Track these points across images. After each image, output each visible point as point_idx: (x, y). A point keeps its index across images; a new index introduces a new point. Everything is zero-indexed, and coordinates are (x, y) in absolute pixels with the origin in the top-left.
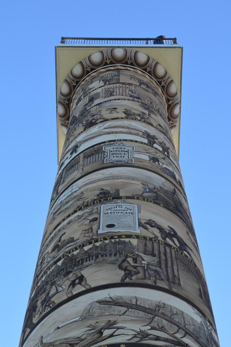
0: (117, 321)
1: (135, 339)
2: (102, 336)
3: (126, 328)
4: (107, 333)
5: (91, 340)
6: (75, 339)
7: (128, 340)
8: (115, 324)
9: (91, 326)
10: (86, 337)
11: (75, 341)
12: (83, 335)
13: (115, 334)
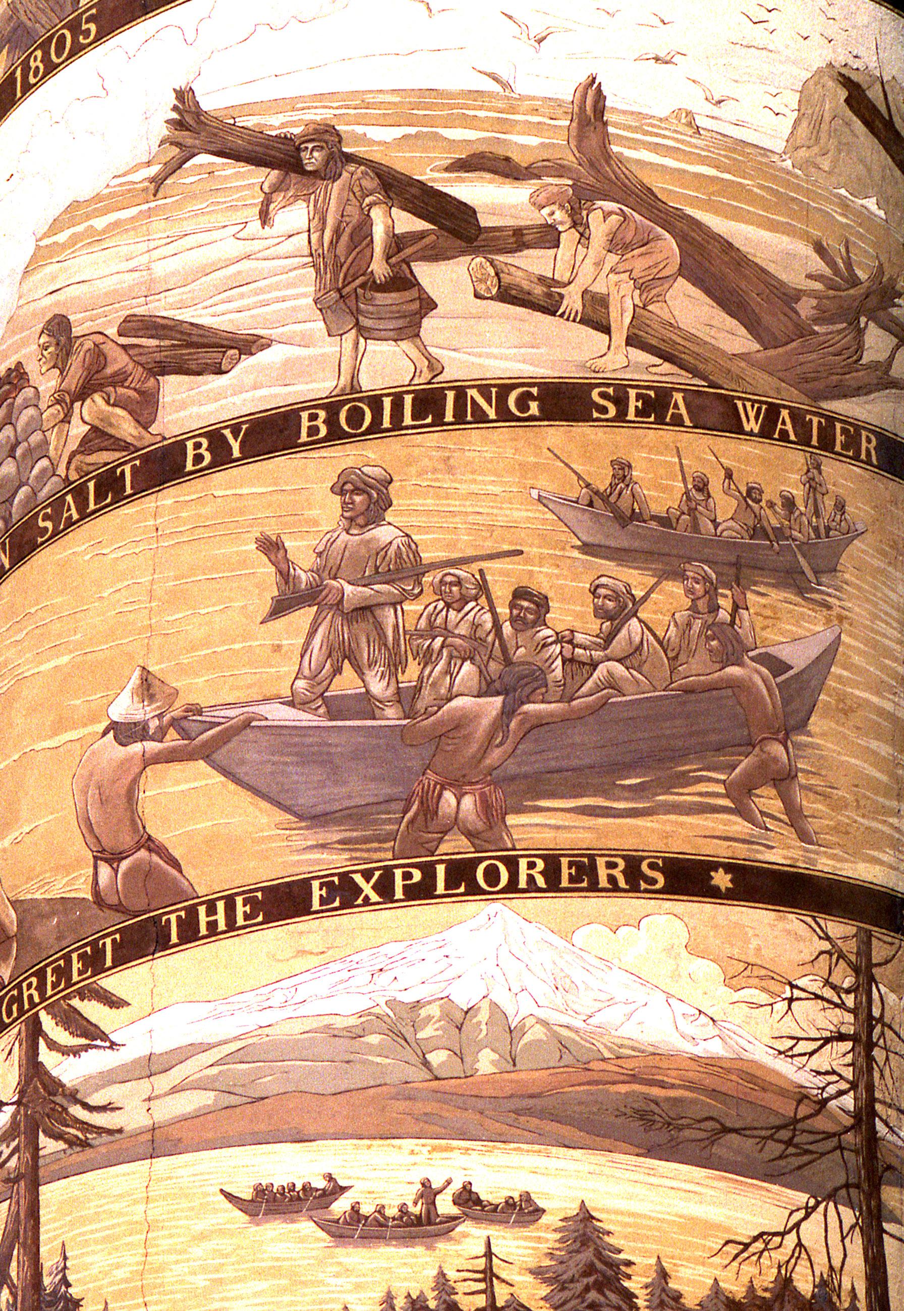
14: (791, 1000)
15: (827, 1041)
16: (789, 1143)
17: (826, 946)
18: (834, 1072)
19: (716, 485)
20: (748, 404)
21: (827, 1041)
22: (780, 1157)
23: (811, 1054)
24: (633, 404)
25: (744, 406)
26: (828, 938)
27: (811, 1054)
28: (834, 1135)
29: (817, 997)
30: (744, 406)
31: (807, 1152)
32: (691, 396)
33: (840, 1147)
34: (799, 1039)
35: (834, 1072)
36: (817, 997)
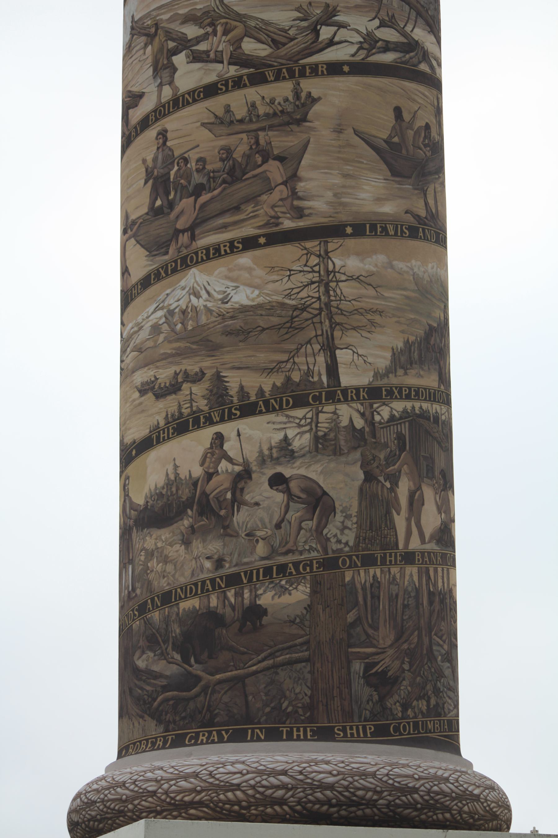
0: (338, 8)
1: (361, 52)
2: (318, 40)
3: (350, 26)
4: (326, 33)
5: (303, 46)
6: (279, 30)
7: (353, 55)
8: (335, 16)
9: (302, 11)
10: (296, 35)
11: (280, 35)
12: (292, 27)
13: (337, 39)
14: (289, 276)
15: (305, 286)
16: (291, 327)
17: (305, 252)
18: (309, 296)
19: (258, 103)
20: (270, 72)
21: (305, 286)
22: (286, 333)
23: (298, 293)
24: (230, 84)
25: (268, 73)
26: (306, 249)
27: (298, 293)
28: (309, 319)
29: (301, 271)
30: (268, 73)
31: (297, 329)
32: (249, 76)
33: (313, 323)
34: (293, 289)
35: (309, 296)
36: (301, 271)
